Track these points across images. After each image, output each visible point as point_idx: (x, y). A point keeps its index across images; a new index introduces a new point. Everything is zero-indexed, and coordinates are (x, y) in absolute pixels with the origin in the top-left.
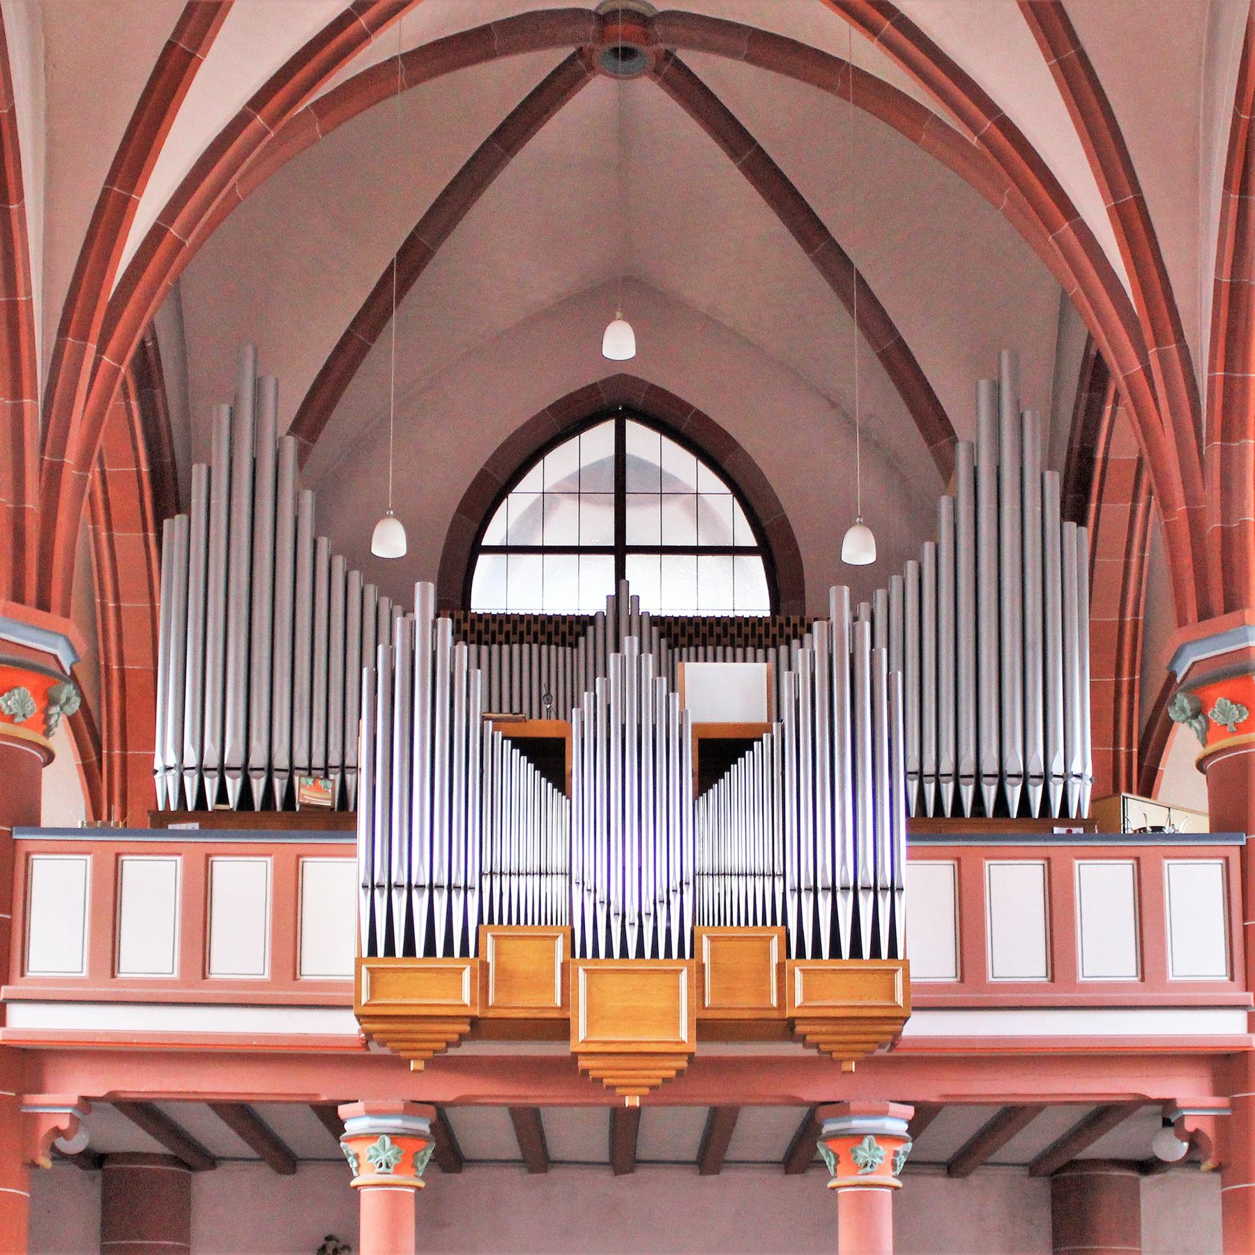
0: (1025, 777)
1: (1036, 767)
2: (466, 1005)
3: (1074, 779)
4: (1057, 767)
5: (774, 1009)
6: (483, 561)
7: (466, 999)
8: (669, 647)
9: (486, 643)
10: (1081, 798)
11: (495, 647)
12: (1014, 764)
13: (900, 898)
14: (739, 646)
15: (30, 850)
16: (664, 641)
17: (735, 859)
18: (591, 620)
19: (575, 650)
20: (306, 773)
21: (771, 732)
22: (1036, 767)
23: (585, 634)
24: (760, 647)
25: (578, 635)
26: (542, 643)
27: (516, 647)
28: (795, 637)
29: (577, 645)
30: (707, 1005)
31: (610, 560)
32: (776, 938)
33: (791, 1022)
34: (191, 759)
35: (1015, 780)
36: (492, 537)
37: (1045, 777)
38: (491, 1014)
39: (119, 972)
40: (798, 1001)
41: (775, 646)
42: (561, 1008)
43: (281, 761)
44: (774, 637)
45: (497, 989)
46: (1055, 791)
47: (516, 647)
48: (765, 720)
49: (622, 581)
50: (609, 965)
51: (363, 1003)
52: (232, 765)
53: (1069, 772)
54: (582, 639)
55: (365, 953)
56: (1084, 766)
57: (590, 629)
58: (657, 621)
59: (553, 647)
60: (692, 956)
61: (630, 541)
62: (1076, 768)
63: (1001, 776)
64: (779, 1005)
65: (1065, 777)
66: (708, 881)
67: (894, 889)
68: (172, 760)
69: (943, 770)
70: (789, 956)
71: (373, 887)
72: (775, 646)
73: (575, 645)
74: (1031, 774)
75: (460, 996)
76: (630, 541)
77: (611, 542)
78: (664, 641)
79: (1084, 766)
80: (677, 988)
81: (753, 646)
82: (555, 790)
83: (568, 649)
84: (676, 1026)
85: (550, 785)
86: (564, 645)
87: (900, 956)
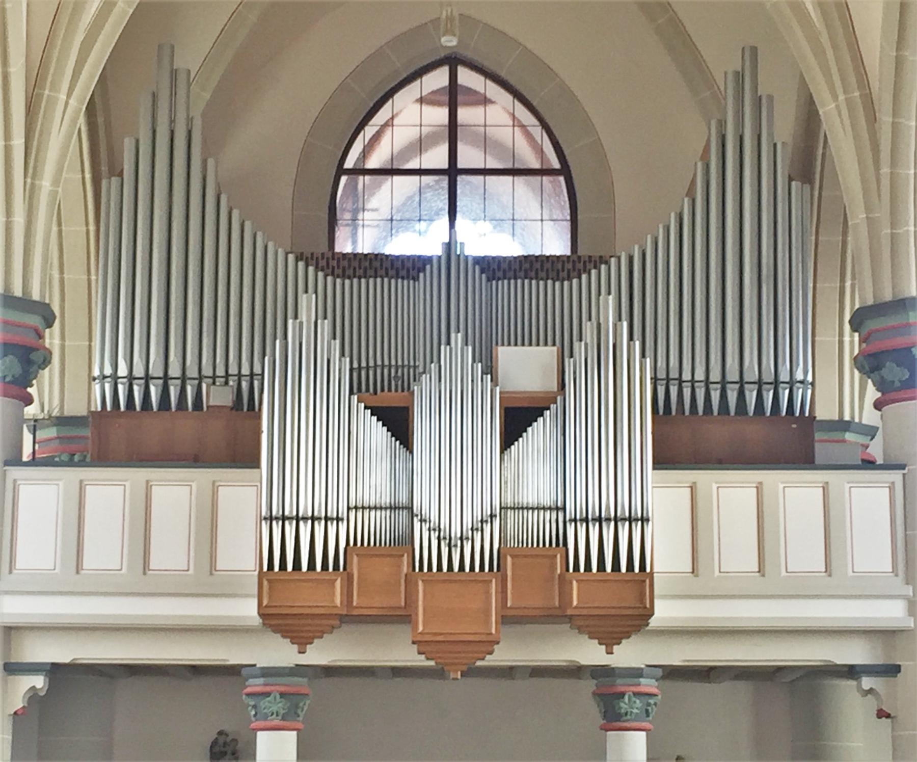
0: (760, 383)
1: (768, 377)
2: (336, 607)
3: (798, 385)
4: (784, 376)
5: (556, 608)
6: (344, 179)
7: (338, 601)
8: (488, 280)
9: (349, 278)
10: (804, 394)
11: (355, 281)
12: (751, 374)
13: (647, 525)
14: (542, 279)
15: (16, 478)
16: (484, 276)
17: (530, 497)
18: (427, 260)
19: (417, 283)
20: (211, 381)
21: (556, 403)
22: (768, 377)
23: (424, 270)
24: (558, 280)
25: (419, 271)
26: (392, 277)
27: (371, 281)
28: (585, 271)
29: (418, 280)
30: (509, 605)
31: (445, 181)
32: (559, 556)
33: (571, 618)
34: (123, 371)
35: (752, 386)
36: (349, 164)
37: (776, 383)
38: (355, 612)
39: (83, 569)
40: (575, 603)
41: (569, 279)
42: (405, 607)
43: (192, 372)
44: (569, 271)
45: (358, 595)
46: (784, 394)
47: (371, 281)
48: (554, 387)
49: (453, 230)
50: (440, 577)
51: (264, 605)
52: (155, 375)
53: (794, 380)
54: (421, 275)
55: (265, 568)
56: (806, 373)
57: (428, 267)
58: (478, 261)
59: (400, 281)
60: (498, 570)
61: (460, 165)
62: (799, 376)
63: (741, 382)
64: (560, 606)
65: (791, 383)
66: (510, 513)
67: (644, 520)
68: (108, 371)
69: (697, 378)
70: (568, 570)
71: (270, 519)
72: (569, 279)
73: (416, 279)
74: (765, 380)
75: (333, 601)
76: (460, 165)
77: (445, 165)
78: (484, 276)
79: (806, 373)
80: (488, 593)
81: (552, 279)
82: (402, 446)
83: (411, 282)
84: (487, 622)
85: (398, 443)
86: (408, 278)
87: (648, 570)
